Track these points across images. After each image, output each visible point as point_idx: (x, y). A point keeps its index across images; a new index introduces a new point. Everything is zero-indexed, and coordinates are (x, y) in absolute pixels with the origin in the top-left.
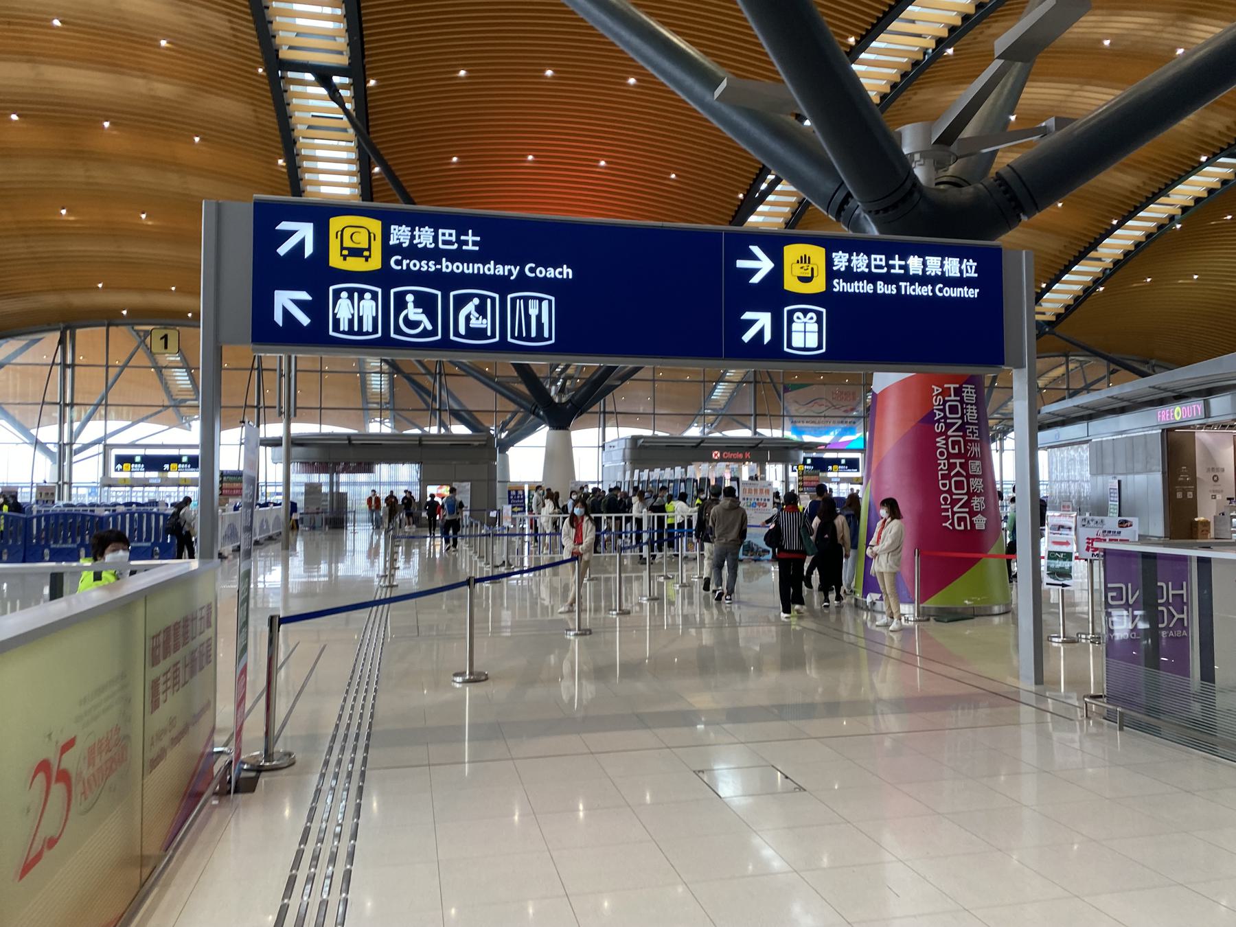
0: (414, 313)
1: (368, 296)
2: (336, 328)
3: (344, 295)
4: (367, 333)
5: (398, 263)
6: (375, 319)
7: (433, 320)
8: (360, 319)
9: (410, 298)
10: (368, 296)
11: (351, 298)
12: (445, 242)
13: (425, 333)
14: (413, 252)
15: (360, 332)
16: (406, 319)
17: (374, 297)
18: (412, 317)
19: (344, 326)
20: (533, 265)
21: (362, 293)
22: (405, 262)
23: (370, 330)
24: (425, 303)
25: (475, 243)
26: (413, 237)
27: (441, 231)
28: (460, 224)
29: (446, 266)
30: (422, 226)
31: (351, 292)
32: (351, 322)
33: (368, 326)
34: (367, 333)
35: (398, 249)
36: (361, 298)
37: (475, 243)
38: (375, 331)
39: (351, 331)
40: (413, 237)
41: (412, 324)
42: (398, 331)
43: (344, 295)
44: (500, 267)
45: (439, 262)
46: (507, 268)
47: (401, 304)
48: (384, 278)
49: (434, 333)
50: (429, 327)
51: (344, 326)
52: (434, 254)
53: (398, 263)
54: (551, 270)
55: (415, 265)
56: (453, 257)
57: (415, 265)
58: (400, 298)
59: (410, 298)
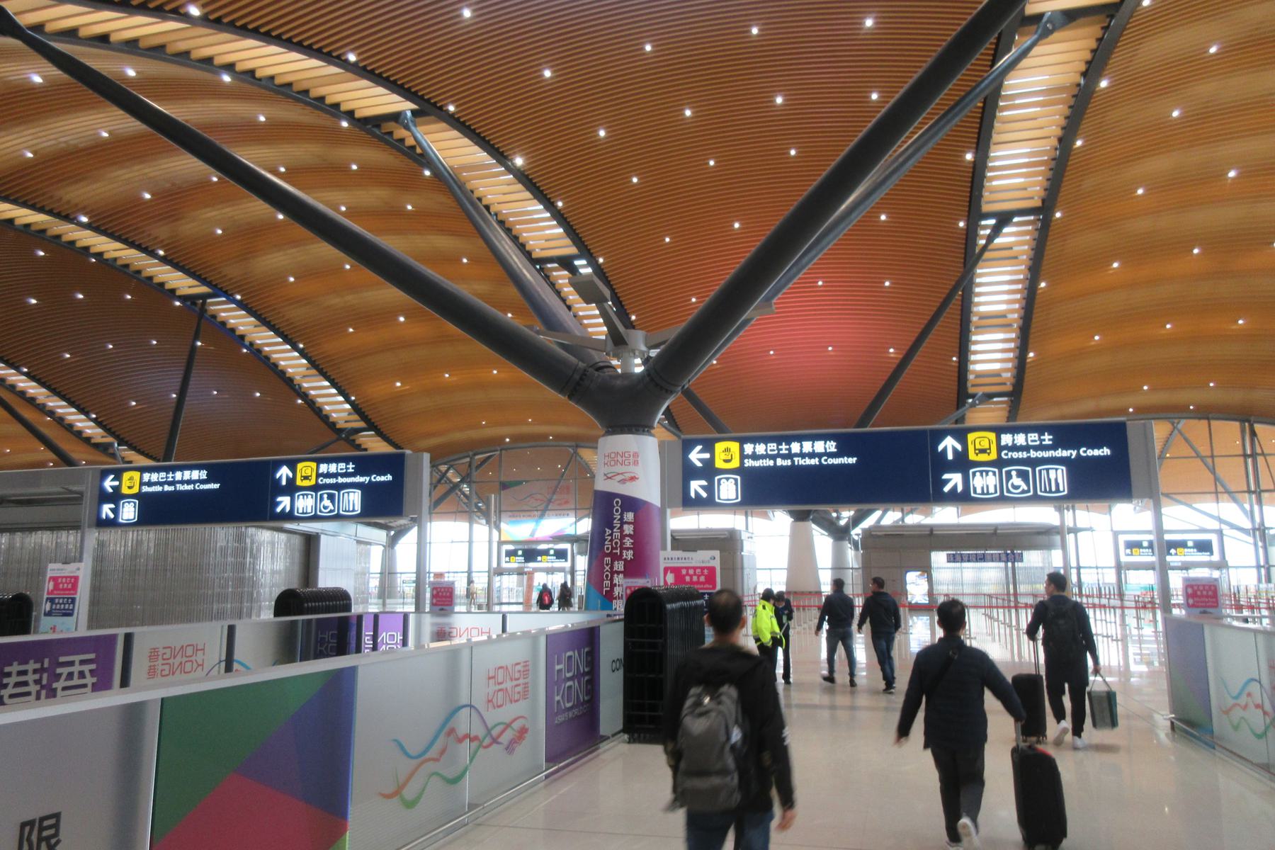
0: (1016, 481)
1: (990, 474)
2: (975, 492)
3: (978, 474)
4: (992, 494)
5: (1006, 454)
6: (996, 486)
7: (1028, 485)
8: (987, 487)
9: (1014, 473)
10: (990, 474)
11: (982, 475)
12: (1032, 441)
13: (1024, 492)
14: (1015, 448)
15: (988, 493)
16: (1013, 485)
17: (994, 473)
18: (1016, 484)
19: (979, 491)
20: (1085, 449)
21: (987, 472)
22: (1010, 454)
23: (993, 492)
24: (1023, 475)
25: (1049, 440)
26: (1014, 440)
27: (1029, 435)
28: (1040, 430)
29: (1033, 454)
30: (1018, 433)
31: (981, 472)
32: (983, 488)
33: (992, 490)
34: (992, 494)
35: (1006, 447)
36: (987, 474)
37: (1049, 440)
38: (996, 492)
39: (983, 493)
40: (1014, 440)
41: (1016, 487)
42: (1008, 491)
43: (978, 474)
44: (1064, 451)
45: (1029, 452)
46: (1069, 452)
47: (1009, 476)
48: (999, 463)
49: (1028, 491)
50: (1026, 488)
51: (979, 491)
52: (1026, 448)
53: (1006, 454)
54: (1096, 451)
55: (1015, 455)
56: (1036, 448)
57: (1015, 455)
58: (1009, 473)
59: (1014, 473)
